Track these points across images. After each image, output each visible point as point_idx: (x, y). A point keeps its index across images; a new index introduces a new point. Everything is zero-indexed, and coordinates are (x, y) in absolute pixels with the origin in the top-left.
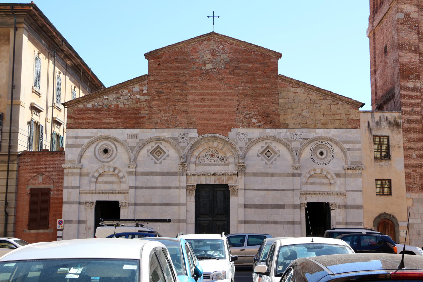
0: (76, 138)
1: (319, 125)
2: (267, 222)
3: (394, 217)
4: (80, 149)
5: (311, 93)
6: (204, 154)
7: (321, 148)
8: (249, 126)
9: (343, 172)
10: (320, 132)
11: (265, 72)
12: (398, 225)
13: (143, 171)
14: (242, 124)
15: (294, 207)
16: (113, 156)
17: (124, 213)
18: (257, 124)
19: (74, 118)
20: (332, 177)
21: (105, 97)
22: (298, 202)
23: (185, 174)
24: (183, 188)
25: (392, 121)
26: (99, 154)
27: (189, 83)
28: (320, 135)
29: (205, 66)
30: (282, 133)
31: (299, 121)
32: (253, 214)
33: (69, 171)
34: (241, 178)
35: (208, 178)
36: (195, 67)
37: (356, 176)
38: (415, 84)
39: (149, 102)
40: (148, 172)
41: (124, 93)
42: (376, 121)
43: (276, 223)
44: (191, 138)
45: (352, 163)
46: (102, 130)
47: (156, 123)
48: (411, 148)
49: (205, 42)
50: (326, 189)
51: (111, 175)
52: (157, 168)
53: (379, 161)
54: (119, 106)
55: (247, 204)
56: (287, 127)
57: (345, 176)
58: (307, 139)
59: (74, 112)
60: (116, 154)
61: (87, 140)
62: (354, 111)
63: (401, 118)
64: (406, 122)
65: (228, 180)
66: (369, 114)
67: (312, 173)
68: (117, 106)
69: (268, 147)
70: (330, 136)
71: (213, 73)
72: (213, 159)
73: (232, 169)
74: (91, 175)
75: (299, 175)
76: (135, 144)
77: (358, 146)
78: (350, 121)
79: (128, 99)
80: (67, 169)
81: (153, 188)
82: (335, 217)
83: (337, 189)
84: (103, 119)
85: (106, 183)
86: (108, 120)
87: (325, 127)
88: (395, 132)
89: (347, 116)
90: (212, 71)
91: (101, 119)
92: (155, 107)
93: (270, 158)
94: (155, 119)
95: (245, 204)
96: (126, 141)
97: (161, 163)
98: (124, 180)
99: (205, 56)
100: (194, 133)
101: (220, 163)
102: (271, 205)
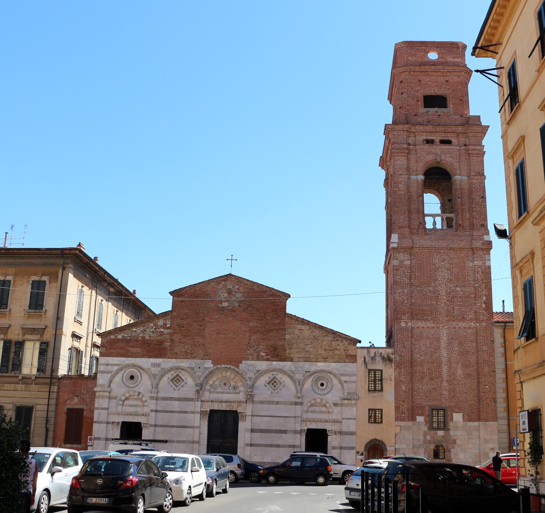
0: (107, 365)
1: (320, 359)
2: (271, 446)
3: (383, 443)
4: (110, 375)
5: (315, 330)
6: (217, 383)
7: (322, 380)
8: (258, 359)
9: (340, 402)
10: (321, 365)
11: (275, 310)
12: (386, 449)
15: (295, 432)
17: (146, 434)
19: (106, 347)
20: (330, 406)
22: (298, 428)
23: (200, 400)
24: (197, 413)
25: (386, 356)
26: (126, 380)
27: (207, 319)
28: (321, 368)
29: (221, 304)
30: (287, 365)
31: (302, 355)
32: (258, 438)
35: (220, 404)
36: (213, 305)
37: (351, 405)
38: (406, 323)
39: (171, 334)
42: (371, 356)
43: (278, 446)
44: (206, 368)
45: (348, 394)
46: (130, 359)
47: (177, 354)
48: (401, 381)
49: (223, 283)
50: (324, 417)
52: (176, 395)
53: (372, 392)
56: (291, 360)
57: (342, 405)
58: (309, 372)
59: (107, 342)
60: (141, 380)
62: (352, 347)
63: (394, 353)
64: (398, 357)
65: (237, 407)
66: (366, 350)
67: (313, 402)
68: (143, 338)
69: (274, 378)
70: (329, 369)
72: (226, 387)
73: (241, 397)
74: (118, 398)
75: (301, 404)
77: (354, 379)
78: (348, 356)
79: (153, 332)
81: (171, 412)
83: (334, 417)
84: (131, 349)
85: (131, 406)
86: (134, 350)
87: (325, 361)
88: (388, 366)
89: (346, 352)
90: (227, 309)
91: (129, 349)
94: (176, 350)
95: (252, 429)
96: (149, 369)
97: (179, 389)
98: (146, 404)
99: (222, 295)
100: (209, 364)
101: (231, 391)
102: (275, 430)
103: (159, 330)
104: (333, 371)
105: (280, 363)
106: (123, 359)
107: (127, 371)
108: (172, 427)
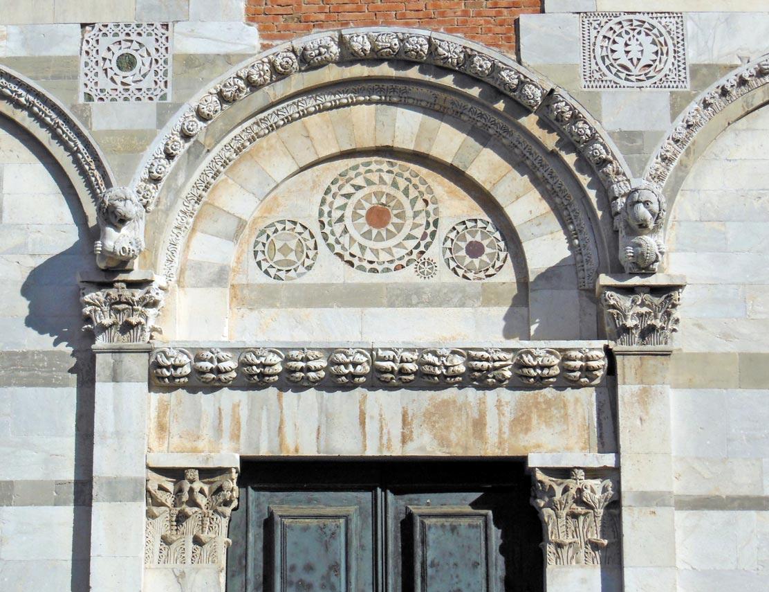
6: (304, 205)
23: (138, 365)
34: (644, 397)
44: (190, 62)
65: (521, 422)
72: (393, 246)
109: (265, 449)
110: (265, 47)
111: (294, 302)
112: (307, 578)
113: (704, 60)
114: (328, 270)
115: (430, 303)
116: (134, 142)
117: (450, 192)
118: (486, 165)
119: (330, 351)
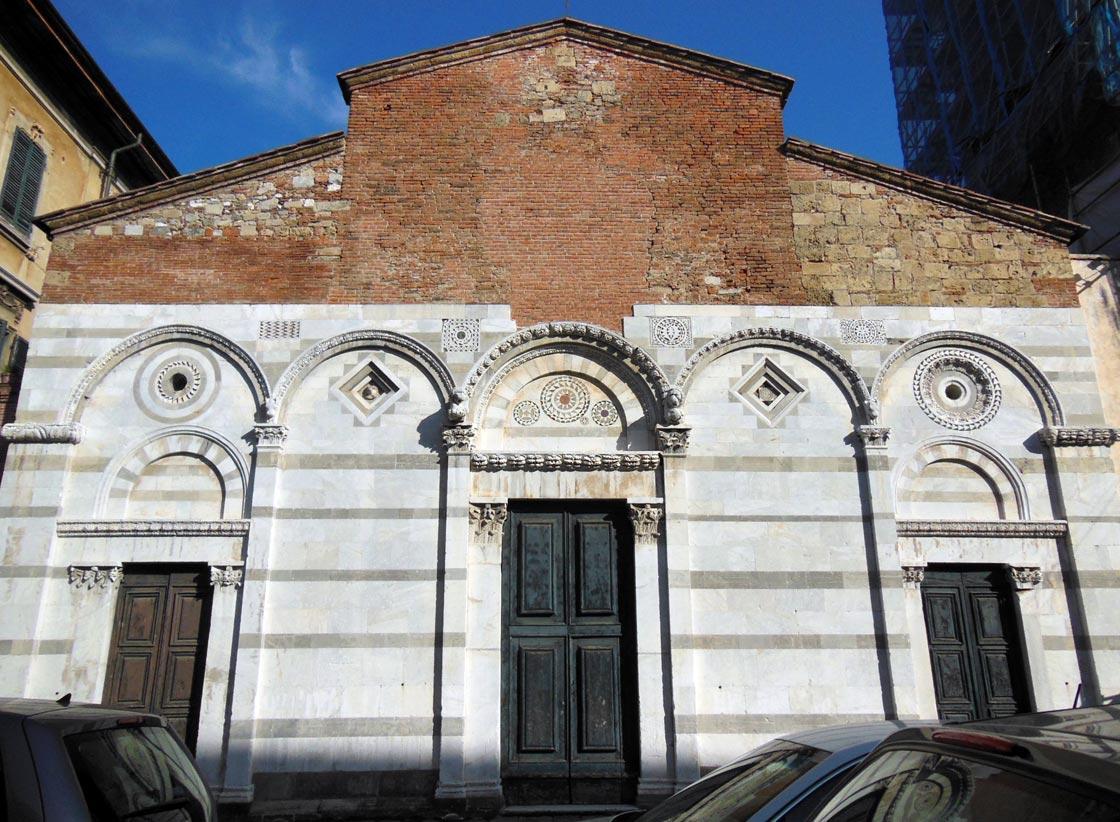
0: (71, 333)
2: (782, 642)
4: (81, 372)
5: (900, 197)
6: (534, 394)
8: (697, 294)
13: (307, 450)
14: (669, 291)
16: (204, 399)
18: (721, 292)
19: (72, 268)
21: (193, 204)
23: (466, 460)
28: (946, 328)
30: (812, 321)
33: (29, 453)
34: (675, 475)
36: (507, 118)
40: (329, 456)
41: (260, 192)
43: (813, 642)
44: (488, 336)
46: (172, 308)
47: (368, 286)
49: (540, 51)
51: (191, 467)
52: (363, 444)
54: (239, 231)
55: (701, 573)
56: (829, 300)
58: (902, 342)
60: (216, 392)
61: (109, 340)
65: (624, 485)
68: (232, 233)
71: (565, 135)
72: (571, 412)
74: (114, 467)
76: (285, 357)
77: (1081, 364)
79: (274, 211)
80: (20, 446)
81: (344, 514)
82: (1035, 616)
85: (170, 496)
86: (194, 276)
87: (959, 302)
89: (1031, 269)
92: (364, 235)
93: (772, 406)
94: (363, 272)
96: (253, 344)
97: (376, 423)
102: (791, 575)
103: (298, 204)
104: (996, 336)
105: (783, 311)
106: (142, 310)
107: (160, 360)
108: (347, 576)
109: (518, 496)
110: (518, 329)
111: (530, 435)
112: (536, 549)
113: (699, 336)
114: (544, 421)
115: (586, 436)
116: (464, 369)
117: (595, 390)
118: (610, 379)
119: (545, 455)
